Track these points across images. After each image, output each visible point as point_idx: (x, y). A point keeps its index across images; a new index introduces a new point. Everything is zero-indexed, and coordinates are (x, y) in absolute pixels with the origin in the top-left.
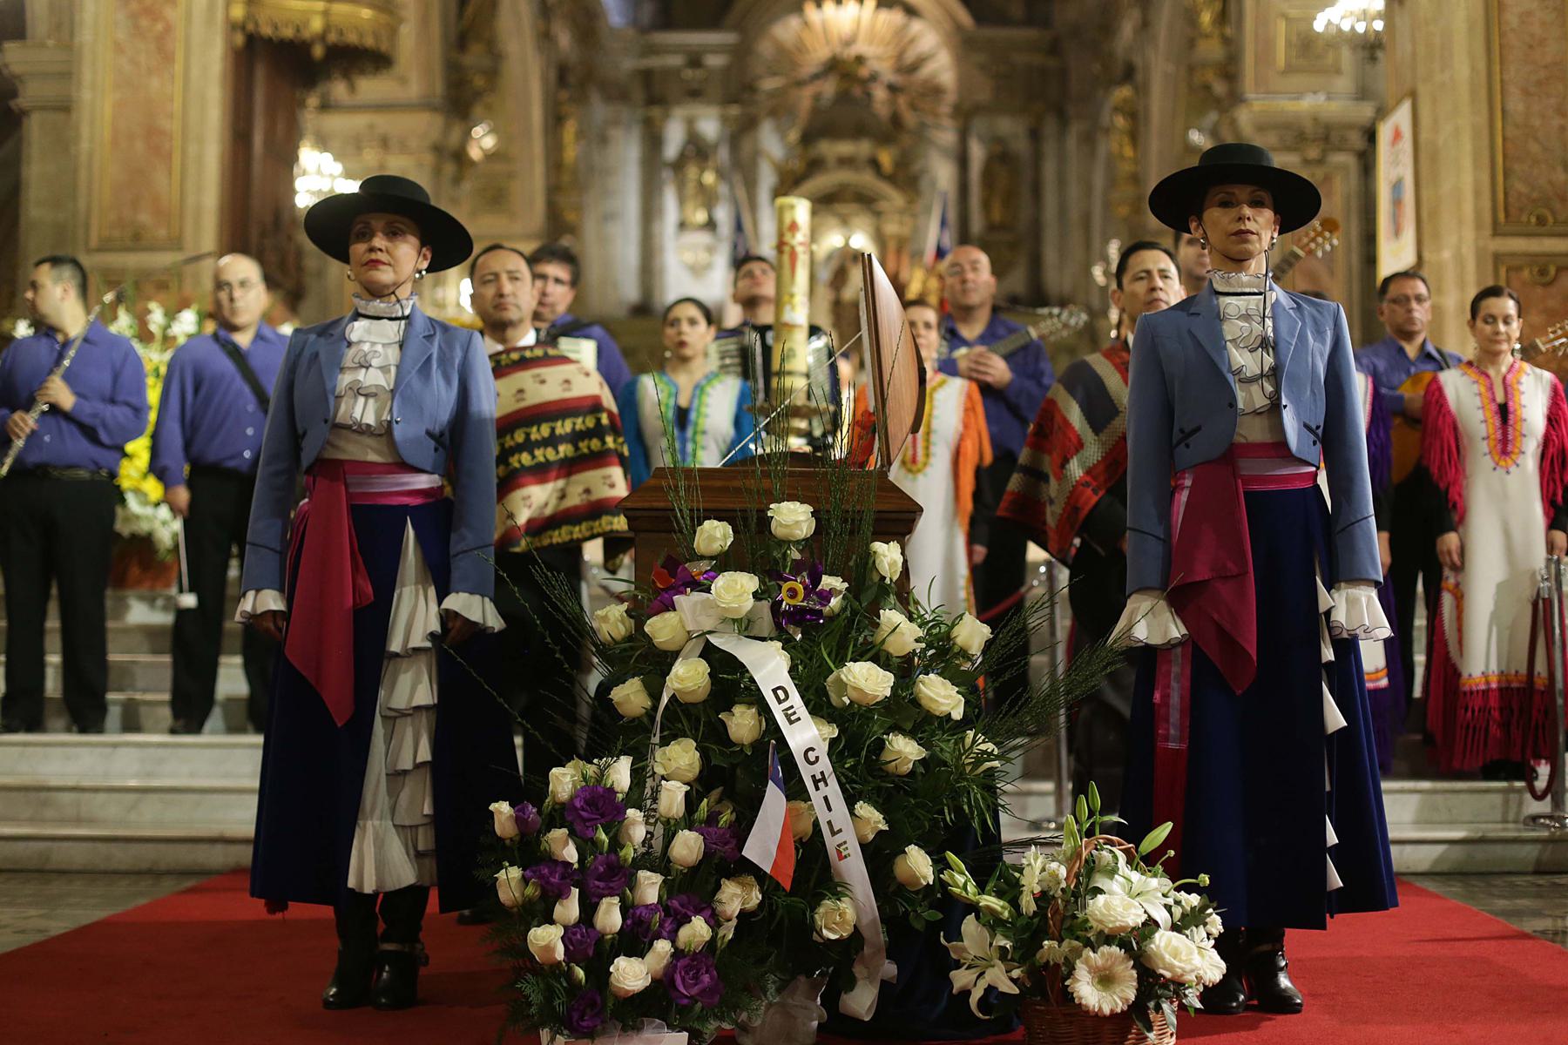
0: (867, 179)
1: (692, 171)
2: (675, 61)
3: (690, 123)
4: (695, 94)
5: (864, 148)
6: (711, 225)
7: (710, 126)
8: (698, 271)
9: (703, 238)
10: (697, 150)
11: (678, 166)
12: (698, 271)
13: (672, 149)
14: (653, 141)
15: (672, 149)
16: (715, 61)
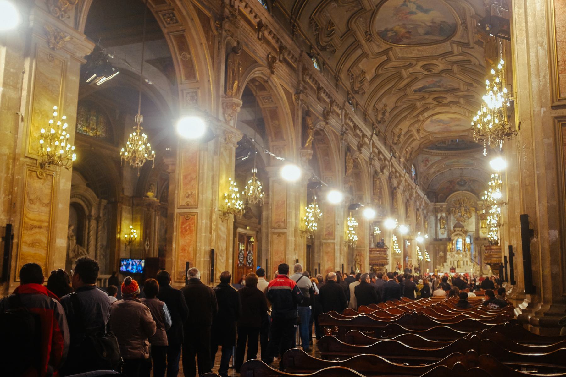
0: (461, 233)
1: (442, 221)
2: (439, 206)
3: (441, 214)
4: (442, 211)
5: (460, 229)
6: (444, 228)
7: (444, 215)
8: (443, 234)
9: (443, 230)
10: (442, 218)
11: (440, 220)
12: (443, 234)
13: (439, 218)
14: (436, 217)
15: (439, 218)
16: (444, 206)
